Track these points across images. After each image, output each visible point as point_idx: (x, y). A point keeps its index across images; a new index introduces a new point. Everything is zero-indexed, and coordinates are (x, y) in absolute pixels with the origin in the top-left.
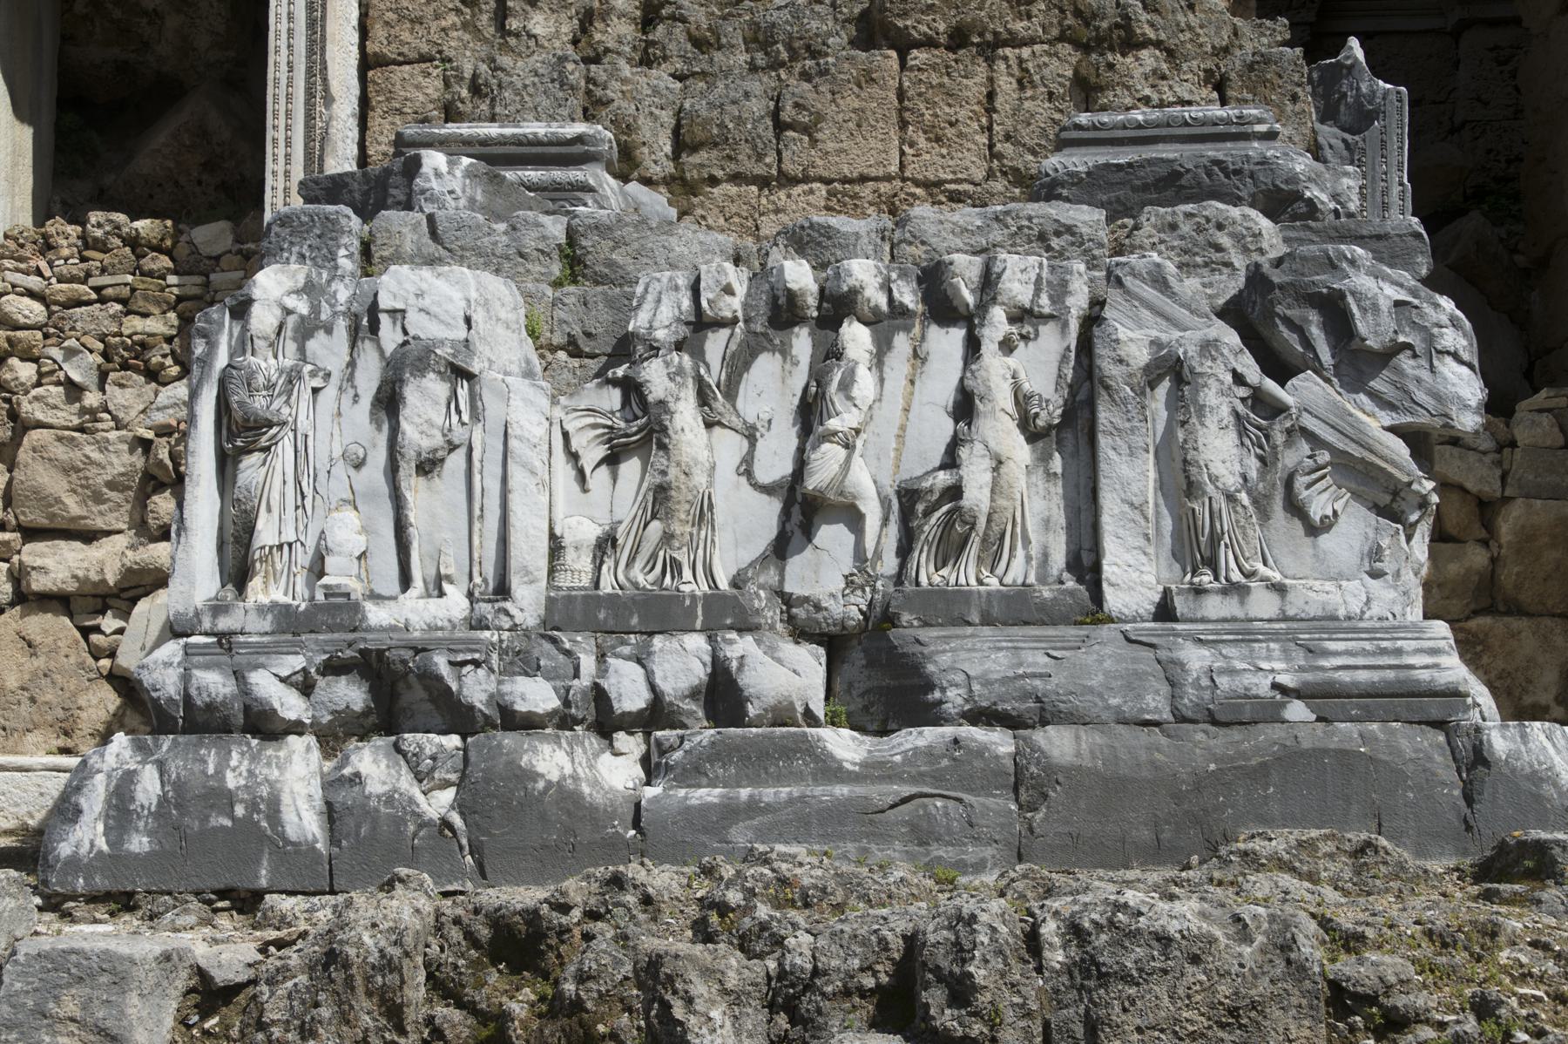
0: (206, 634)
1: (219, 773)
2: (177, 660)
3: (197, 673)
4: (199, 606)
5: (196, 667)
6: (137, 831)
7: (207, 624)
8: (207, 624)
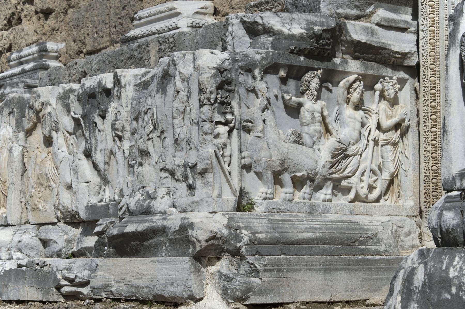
0: (458, 190)
1: (448, 269)
2: (440, 205)
3: (445, 213)
4: (454, 174)
5: (446, 210)
6: (413, 300)
7: (458, 185)
8: (458, 185)
